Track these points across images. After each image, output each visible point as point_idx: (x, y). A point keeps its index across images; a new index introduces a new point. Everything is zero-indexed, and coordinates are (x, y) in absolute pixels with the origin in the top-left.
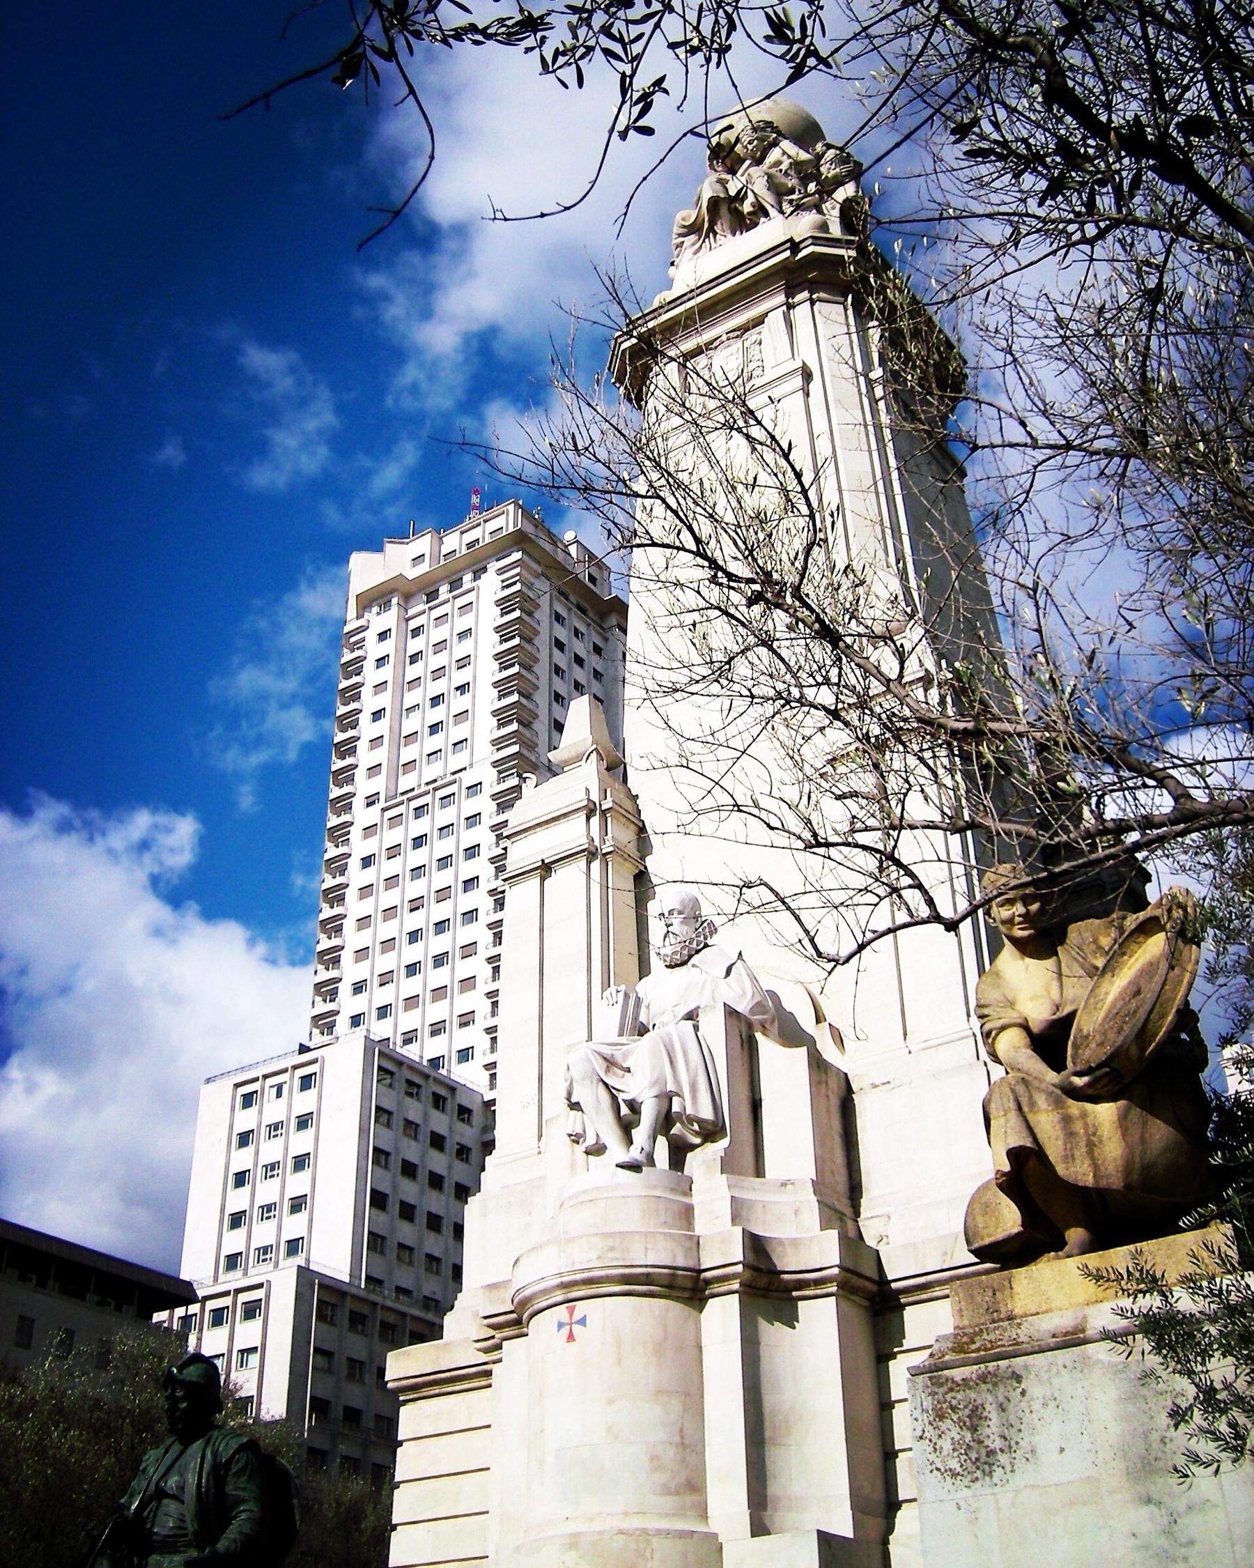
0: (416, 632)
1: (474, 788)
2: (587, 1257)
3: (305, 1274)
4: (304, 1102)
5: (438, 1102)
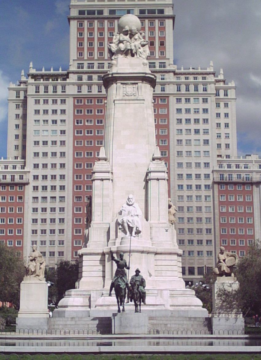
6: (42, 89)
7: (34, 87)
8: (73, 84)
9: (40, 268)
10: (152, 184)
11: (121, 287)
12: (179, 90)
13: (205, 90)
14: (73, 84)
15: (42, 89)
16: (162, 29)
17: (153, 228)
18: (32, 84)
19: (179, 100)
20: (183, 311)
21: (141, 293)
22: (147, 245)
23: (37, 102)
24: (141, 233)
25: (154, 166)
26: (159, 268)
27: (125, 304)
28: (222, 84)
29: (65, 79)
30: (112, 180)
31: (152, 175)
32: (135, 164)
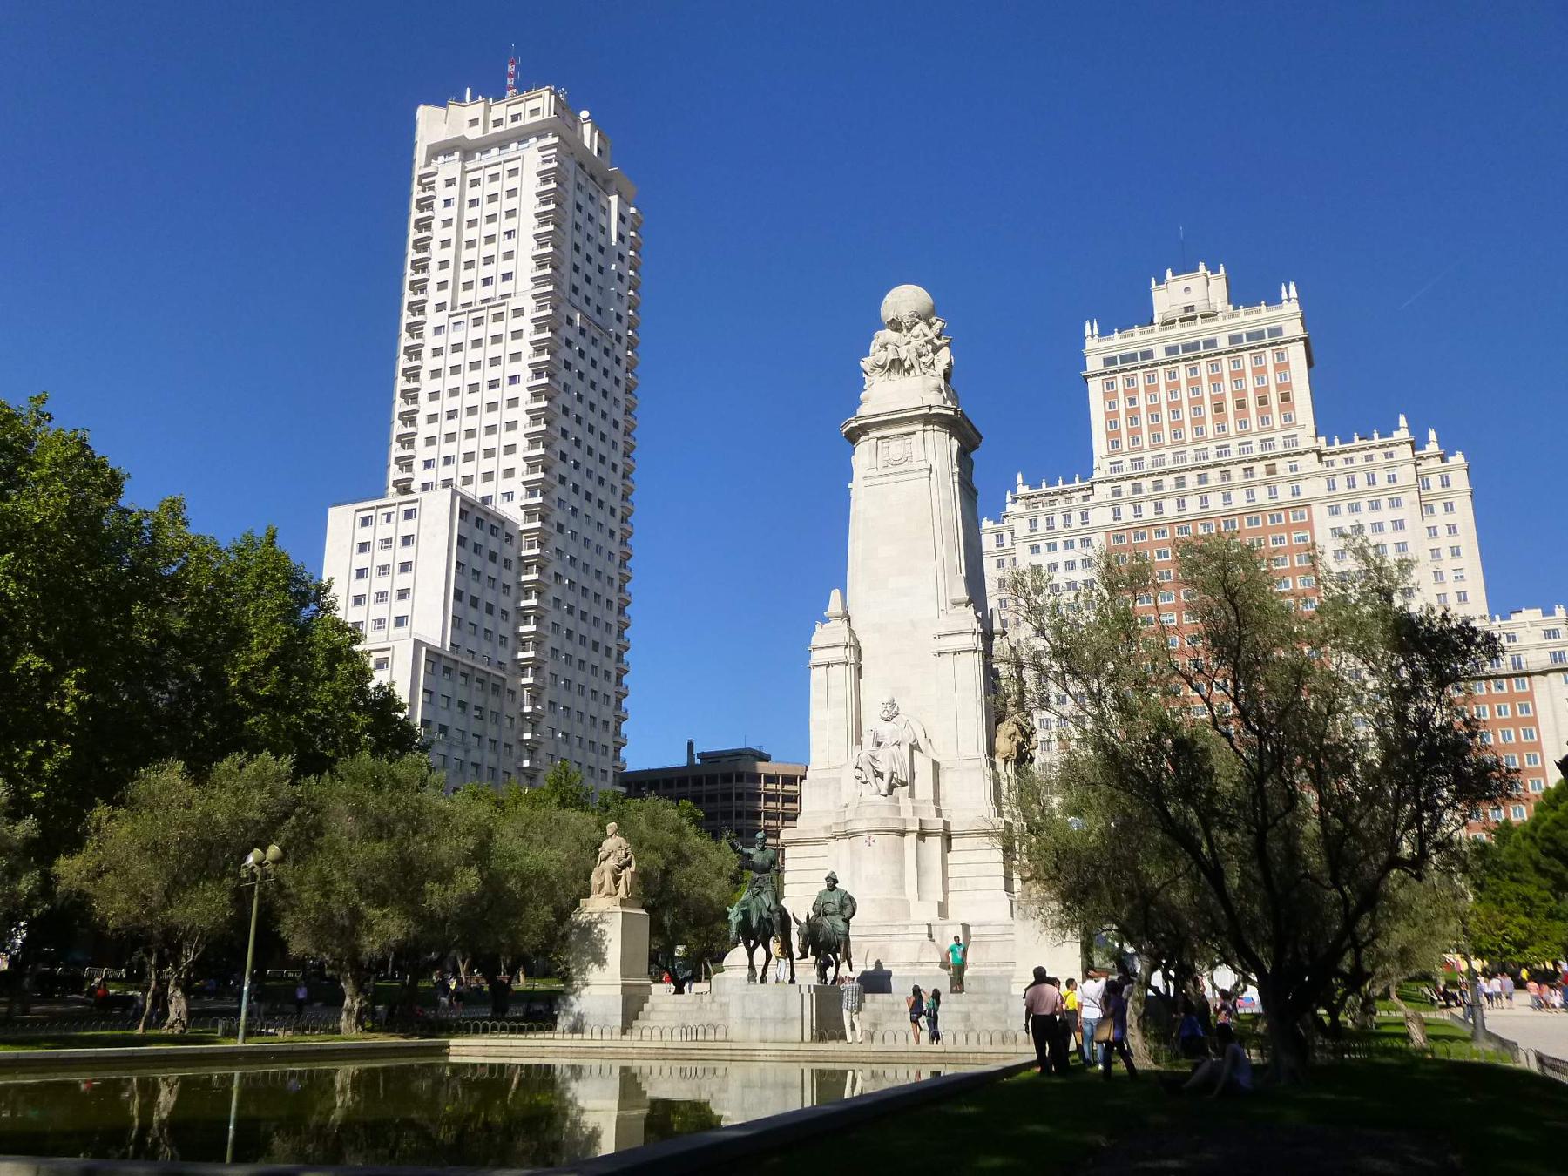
0: (475, 183)
1: (518, 312)
2: (875, 825)
3: (418, 644)
4: (408, 527)
5: (493, 530)
6: (1042, 523)
7: (1026, 521)
8: (1102, 504)
9: (616, 880)
12: (1332, 487)
13: (1392, 479)
14: (1102, 504)
15: (1042, 523)
16: (1282, 367)
18: (1021, 516)
19: (1334, 511)
20: (995, 978)
23: (1035, 549)
28: (1435, 463)
29: (1086, 498)
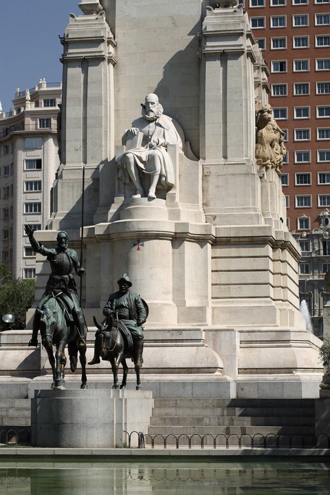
10: (213, 68)
11: (42, 319)
17: (210, 179)
21: (130, 338)
22: (194, 220)
24: (170, 192)
25: (215, 21)
26: (224, 278)
27: (87, 366)
30: (110, 60)
31: (211, 46)
32: (172, 18)
